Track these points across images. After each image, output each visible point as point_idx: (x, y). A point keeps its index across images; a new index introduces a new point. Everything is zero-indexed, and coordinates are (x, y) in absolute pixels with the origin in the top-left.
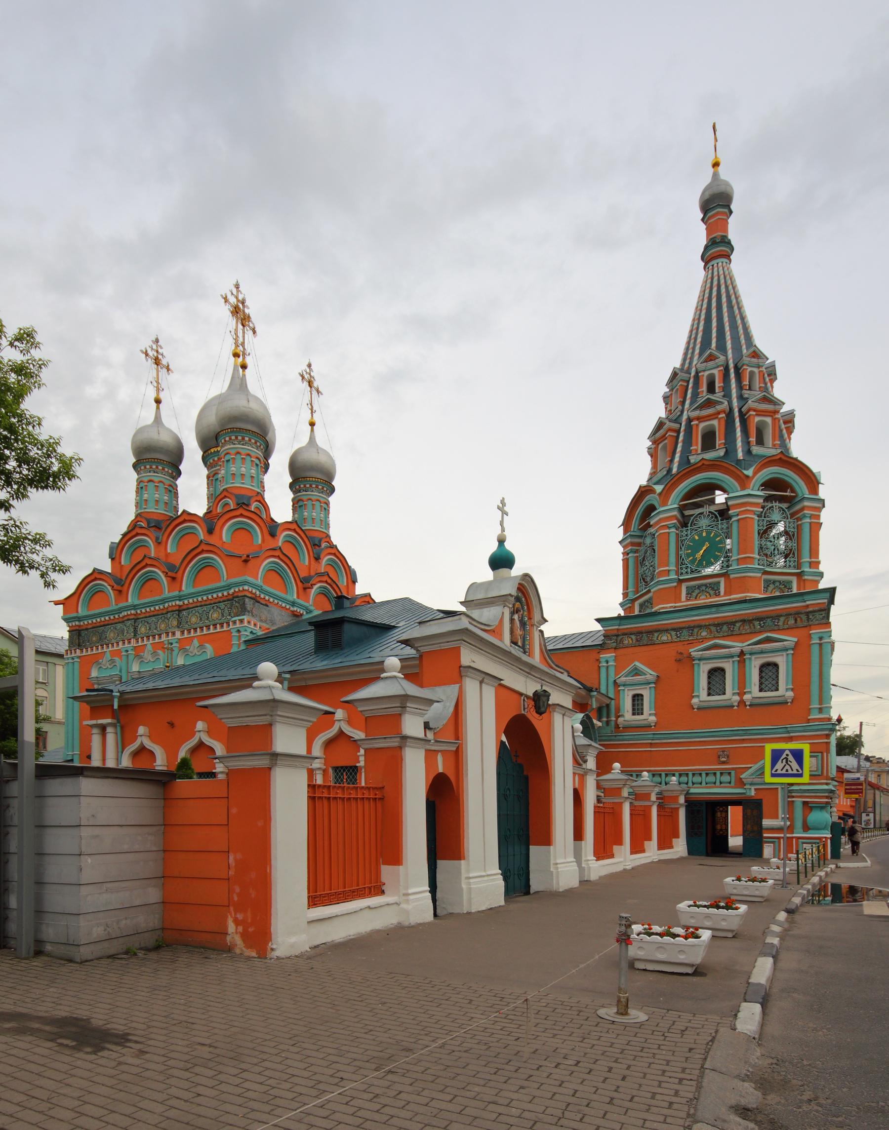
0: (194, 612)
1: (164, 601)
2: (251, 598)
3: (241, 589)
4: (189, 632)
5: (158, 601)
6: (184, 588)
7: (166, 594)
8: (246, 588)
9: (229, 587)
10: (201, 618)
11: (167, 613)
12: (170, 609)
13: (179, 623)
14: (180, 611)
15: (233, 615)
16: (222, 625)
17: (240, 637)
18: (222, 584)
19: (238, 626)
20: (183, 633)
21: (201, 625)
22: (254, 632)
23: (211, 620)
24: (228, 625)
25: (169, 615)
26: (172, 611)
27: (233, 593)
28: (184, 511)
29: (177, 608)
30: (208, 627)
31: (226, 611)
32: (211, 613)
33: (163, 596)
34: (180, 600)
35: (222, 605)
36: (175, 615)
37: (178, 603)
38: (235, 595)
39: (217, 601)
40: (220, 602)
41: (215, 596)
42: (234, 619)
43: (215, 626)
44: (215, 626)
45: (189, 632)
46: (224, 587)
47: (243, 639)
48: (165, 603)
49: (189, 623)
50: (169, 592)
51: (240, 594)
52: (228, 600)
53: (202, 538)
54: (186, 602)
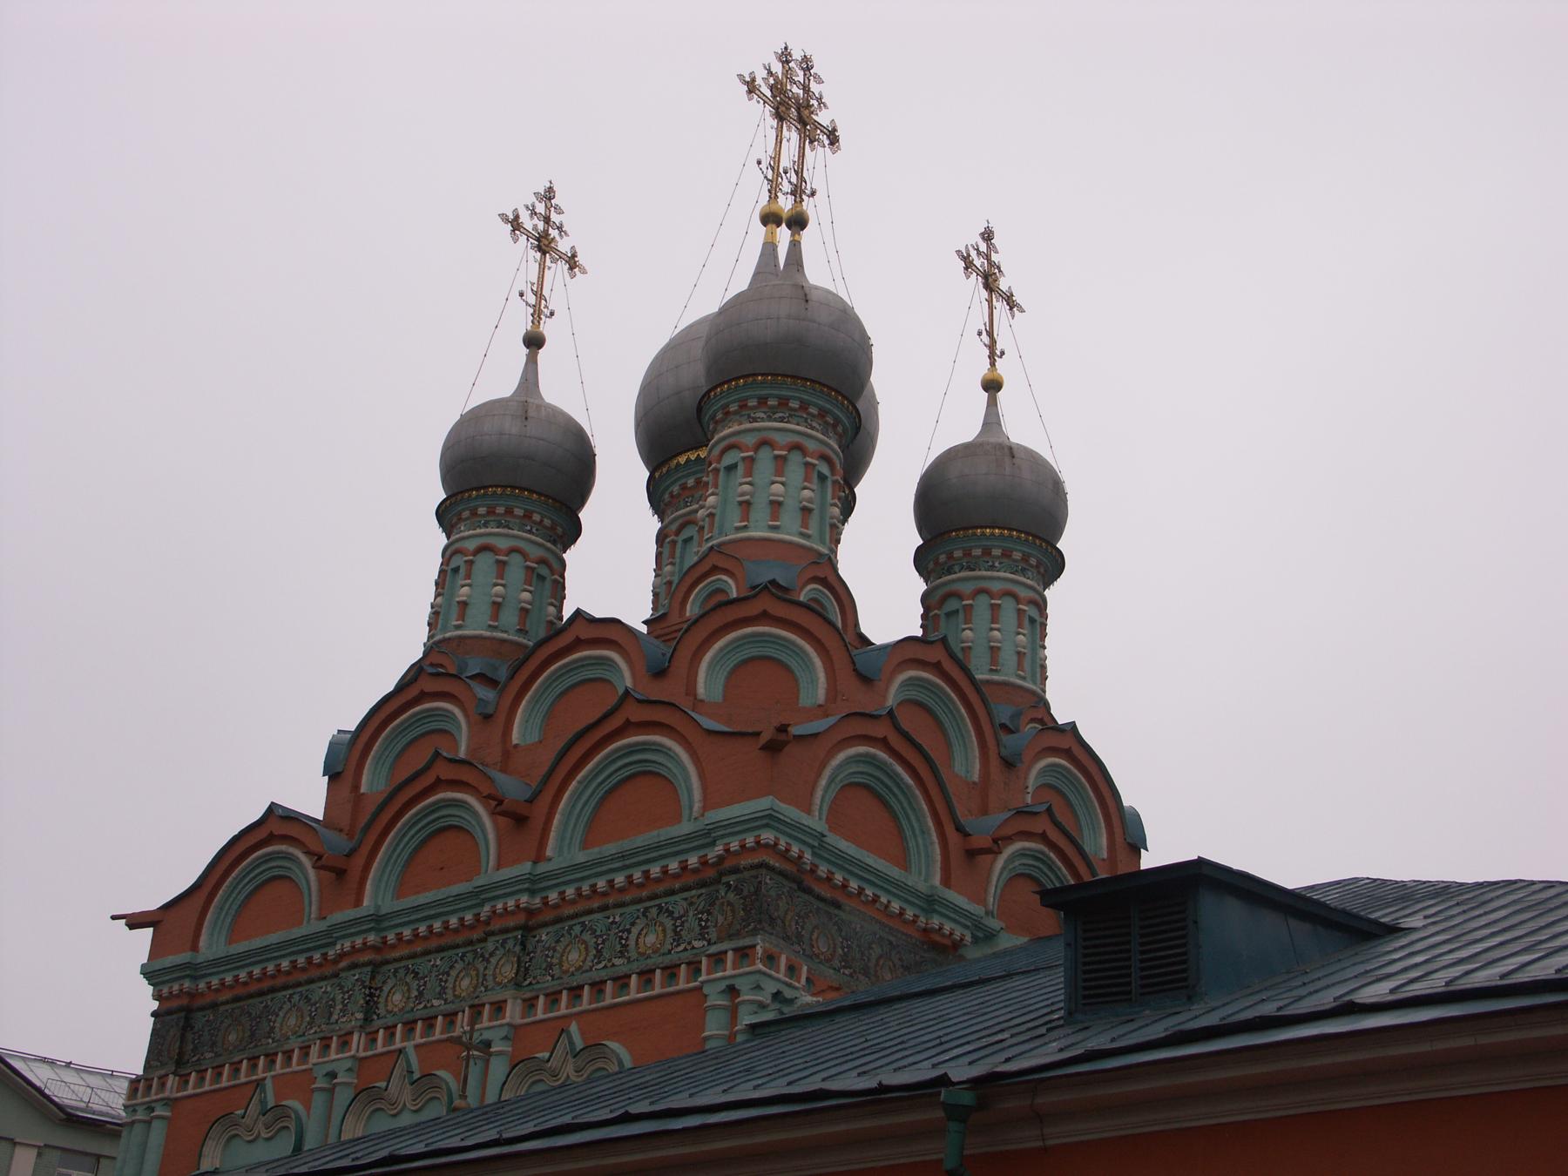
0: (577, 929)
1: (479, 896)
2: (782, 873)
3: (750, 841)
4: (553, 998)
5: (459, 897)
6: (549, 853)
7: (490, 873)
8: (767, 836)
9: (707, 836)
10: (599, 952)
11: (484, 940)
12: (496, 925)
13: (523, 971)
14: (527, 929)
15: (714, 936)
16: (671, 971)
17: (733, 1012)
18: (685, 828)
19: (729, 972)
20: (530, 1004)
21: (595, 976)
22: (788, 993)
23: (633, 955)
24: (695, 967)
25: (490, 946)
26: (506, 931)
27: (721, 859)
28: (578, 614)
29: (521, 919)
30: (622, 981)
31: (691, 921)
32: (635, 931)
33: (480, 881)
34: (532, 892)
35: (678, 903)
36: (510, 944)
37: (524, 899)
38: (727, 864)
39: (661, 888)
40: (672, 893)
41: (655, 870)
42: (713, 949)
43: (646, 975)
44: (646, 975)
45: (553, 998)
46: (688, 838)
47: (746, 1019)
48: (481, 905)
49: (556, 971)
50: (499, 866)
51: (745, 861)
52: (703, 884)
53: (629, 683)
54: (553, 896)
